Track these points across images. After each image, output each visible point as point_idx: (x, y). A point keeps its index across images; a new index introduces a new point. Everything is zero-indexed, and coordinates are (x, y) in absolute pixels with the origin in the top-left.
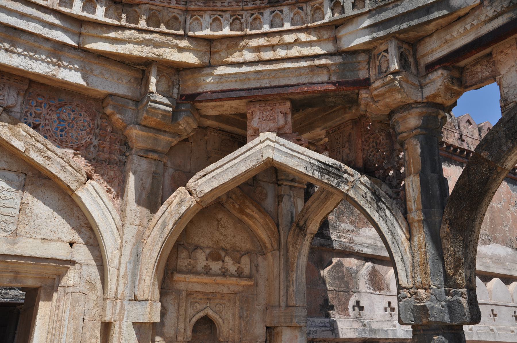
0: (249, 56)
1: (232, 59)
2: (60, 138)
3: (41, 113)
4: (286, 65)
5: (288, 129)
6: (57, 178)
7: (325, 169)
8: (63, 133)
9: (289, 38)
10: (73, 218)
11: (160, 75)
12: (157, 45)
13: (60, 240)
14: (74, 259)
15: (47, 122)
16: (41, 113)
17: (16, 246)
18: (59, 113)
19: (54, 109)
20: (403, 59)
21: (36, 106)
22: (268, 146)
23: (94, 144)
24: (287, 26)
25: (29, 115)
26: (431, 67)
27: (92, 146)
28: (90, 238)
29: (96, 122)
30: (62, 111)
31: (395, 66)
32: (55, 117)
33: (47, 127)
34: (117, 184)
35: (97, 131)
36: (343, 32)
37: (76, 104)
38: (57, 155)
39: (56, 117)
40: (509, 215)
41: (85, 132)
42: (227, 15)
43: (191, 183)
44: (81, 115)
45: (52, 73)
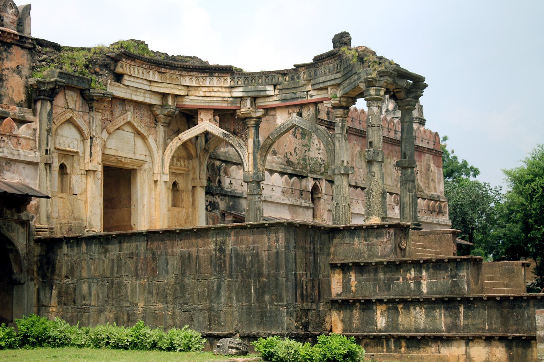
0: (202, 94)
4: (215, 99)
7: (225, 135)
9: (216, 89)
12: (172, 88)
20: (251, 103)
26: (260, 107)
31: (249, 106)
36: (234, 90)
40: (288, 139)
42: (194, 78)
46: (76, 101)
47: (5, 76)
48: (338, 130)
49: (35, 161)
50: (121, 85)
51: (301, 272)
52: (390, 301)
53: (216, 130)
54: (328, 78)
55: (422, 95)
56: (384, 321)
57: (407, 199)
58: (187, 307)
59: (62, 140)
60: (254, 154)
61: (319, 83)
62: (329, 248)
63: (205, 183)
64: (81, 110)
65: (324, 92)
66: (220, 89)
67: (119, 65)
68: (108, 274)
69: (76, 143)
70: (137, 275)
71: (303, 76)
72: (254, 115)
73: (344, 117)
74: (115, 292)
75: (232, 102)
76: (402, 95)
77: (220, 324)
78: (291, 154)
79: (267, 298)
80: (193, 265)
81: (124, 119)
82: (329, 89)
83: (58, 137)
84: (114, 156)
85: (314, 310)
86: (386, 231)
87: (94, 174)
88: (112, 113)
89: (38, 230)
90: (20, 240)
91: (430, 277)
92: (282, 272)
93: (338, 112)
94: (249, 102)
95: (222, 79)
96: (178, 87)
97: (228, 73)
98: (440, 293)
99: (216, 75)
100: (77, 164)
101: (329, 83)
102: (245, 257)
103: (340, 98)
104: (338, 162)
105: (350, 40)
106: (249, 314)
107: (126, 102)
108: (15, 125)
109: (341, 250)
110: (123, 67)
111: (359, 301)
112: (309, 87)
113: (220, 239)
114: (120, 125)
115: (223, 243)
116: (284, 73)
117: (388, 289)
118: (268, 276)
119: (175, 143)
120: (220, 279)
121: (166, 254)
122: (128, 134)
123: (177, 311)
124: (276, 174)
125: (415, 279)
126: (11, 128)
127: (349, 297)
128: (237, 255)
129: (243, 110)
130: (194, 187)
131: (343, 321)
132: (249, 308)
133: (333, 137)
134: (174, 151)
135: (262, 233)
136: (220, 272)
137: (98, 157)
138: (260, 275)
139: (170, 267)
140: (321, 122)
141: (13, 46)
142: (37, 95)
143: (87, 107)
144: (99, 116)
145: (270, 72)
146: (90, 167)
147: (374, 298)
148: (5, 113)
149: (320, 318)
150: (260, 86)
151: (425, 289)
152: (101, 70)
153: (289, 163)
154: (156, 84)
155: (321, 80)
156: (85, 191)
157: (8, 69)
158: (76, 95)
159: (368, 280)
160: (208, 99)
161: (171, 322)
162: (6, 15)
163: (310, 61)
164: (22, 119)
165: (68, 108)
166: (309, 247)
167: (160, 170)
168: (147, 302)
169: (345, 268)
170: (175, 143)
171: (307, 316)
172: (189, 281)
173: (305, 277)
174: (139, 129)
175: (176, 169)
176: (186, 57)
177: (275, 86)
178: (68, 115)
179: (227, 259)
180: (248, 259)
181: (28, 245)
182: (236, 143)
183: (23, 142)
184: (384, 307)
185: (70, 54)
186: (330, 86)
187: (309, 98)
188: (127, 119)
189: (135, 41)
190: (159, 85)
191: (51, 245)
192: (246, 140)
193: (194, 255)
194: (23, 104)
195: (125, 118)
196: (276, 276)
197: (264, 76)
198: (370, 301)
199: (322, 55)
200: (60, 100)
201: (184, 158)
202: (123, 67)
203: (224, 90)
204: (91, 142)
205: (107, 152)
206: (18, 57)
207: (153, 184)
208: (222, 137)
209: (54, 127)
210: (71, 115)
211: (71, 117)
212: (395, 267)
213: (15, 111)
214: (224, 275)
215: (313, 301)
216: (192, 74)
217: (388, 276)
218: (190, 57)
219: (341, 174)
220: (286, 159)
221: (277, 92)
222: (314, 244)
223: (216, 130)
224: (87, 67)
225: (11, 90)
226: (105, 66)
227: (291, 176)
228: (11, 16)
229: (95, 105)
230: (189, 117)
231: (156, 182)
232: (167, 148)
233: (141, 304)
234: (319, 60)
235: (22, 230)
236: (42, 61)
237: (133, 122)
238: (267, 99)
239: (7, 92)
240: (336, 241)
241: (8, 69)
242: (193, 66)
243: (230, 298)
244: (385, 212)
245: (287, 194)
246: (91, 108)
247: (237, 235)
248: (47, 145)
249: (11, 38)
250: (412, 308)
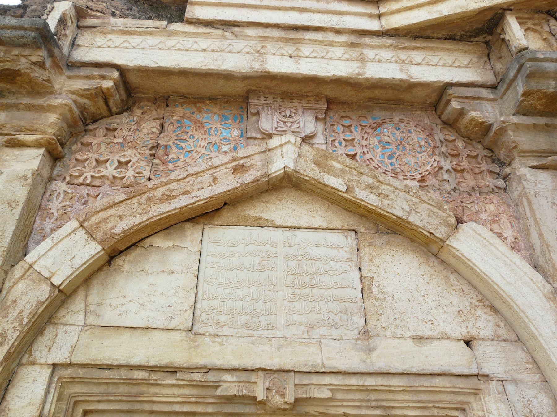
2: (391, 168)
3: (353, 139)
6: (408, 223)
8: (394, 160)
10: (453, 293)
13: (444, 337)
14: (485, 371)
15: (365, 150)
16: (353, 139)
17: (374, 354)
18: (379, 135)
19: (369, 130)
21: (343, 132)
23: (445, 168)
25: (337, 144)
27: (443, 171)
28: (498, 326)
29: (436, 137)
30: (382, 132)
32: (374, 141)
33: (368, 157)
34: (509, 224)
35: (443, 149)
37: (398, 119)
38: (396, 189)
39: (376, 141)
41: (425, 154)
44: (411, 133)
45: (357, 72)
84: (172, 370)
107: (253, 101)
188: (268, 162)
195: (257, 160)
237: (310, 171)
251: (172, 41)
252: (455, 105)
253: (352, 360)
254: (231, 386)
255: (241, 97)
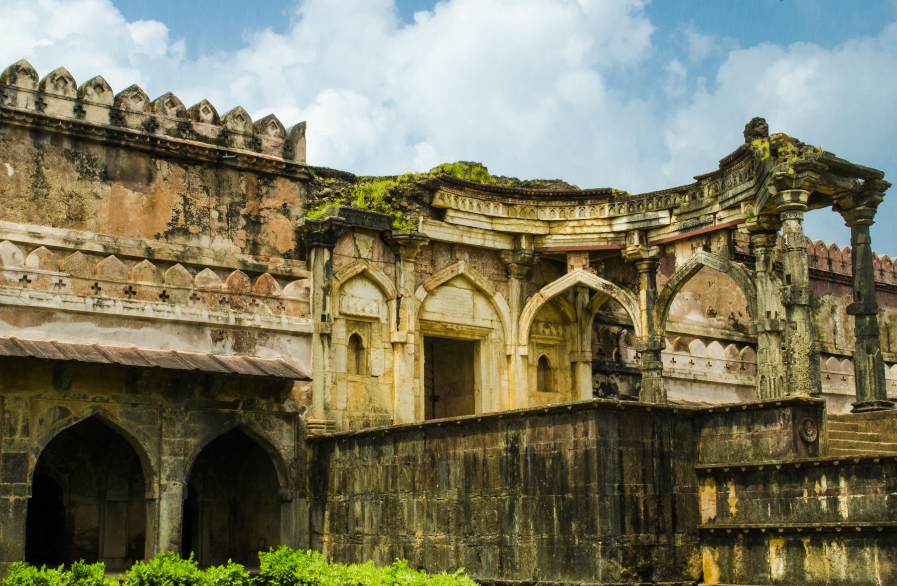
0: (569, 230)
1: (561, 232)
4: (588, 236)
5: (588, 266)
7: (606, 286)
9: (589, 223)
11: (526, 239)
20: (641, 240)
22: (580, 273)
24: (588, 217)
26: (653, 243)
36: (614, 222)
40: (735, 294)
42: (558, 209)
43: (542, 291)
46: (372, 248)
47: (264, 217)
48: (759, 267)
49: (306, 331)
50: (444, 224)
51: (633, 484)
52: (788, 532)
53: (594, 280)
54: (740, 188)
55: (882, 201)
56: (782, 566)
57: (867, 365)
58: (473, 540)
59: (352, 302)
60: (648, 311)
61: (729, 199)
62: (695, 444)
63: (589, 356)
64: (381, 259)
65: (737, 211)
66: (595, 223)
67: (438, 195)
68: (382, 486)
69: (375, 305)
70: (414, 490)
71: (708, 192)
72: (645, 255)
73: (769, 246)
74: (390, 517)
75: (614, 240)
76: (848, 202)
77: (513, 567)
78: (741, 315)
79: (574, 526)
80: (479, 473)
81: (452, 271)
82: (742, 205)
83: (345, 298)
84: (439, 322)
85: (664, 545)
86: (780, 412)
87: (403, 347)
88: (433, 263)
89: (310, 426)
90: (284, 442)
91: (853, 489)
92: (594, 484)
93: (758, 240)
94: (636, 237)
95: (597, 208)
96: (534, 223)
97: (605, 198)
98: (870, 518)
99: (589, 202)
100: (377, 334)
101: (741, 197)
102: (543, 460)
103: (758, 217)
104: (762, 314)
105: (766, 129)
106: (551, 552)
107: (456, 248)
108: (276, 283)
109: (713, 446)
110: (445, 198)
111: (741, 530)
112: (717, 207)
113: (511, 433)
114: (446, 279)
115: (516, 439)
116: (681, 191)
117: (787, 512)
118: (575, 491)
119: (535, 303)
120: (513, 496)
121: (448, 455)
122: (461, 291)
123: (462, 545)
124: (715, 344)
125: (828, 493)
126: (269, 287)
127: (728, 523)
128: (534, 456)
129: (630, 249)
130: (574, 364)
131: (719, 564)
132: (551, 541)
133: (755, 276)
134: (534, 312)
135: (565, 421)
136: (512, 485)
137: (410, 323)
138: (564, 489)
139: (452, 478)
140: (739, 257)
141: (278, 178)
142: (313, 240)
143: (392, 256)
144: (410, 267)
145: (663, 192)
146: (396, 338)
147: (764, 525)
148: (261, 267)
149: (676, 559)
150: (650, 213)
151: (844, 511)
152: (409, 204)
153: (738, 327)
154: (500, 221)
155: (730, 193)
156: (391, 371)
157: (268, 208)
158: (371, 241)
159: (754, 495)
160: (579, 237)
161: (453, 562)
162: (266, 137)
163: (716, 168)
164: (287, 274)
165: (360, 257)
166: (650, 441)
167: (514, 340)
168: (426, 530)
169: (719, 477)
170: (535, 303)
171: (647, 556)
172: (475, 498)
173: (642, 492)
174: (478, 283)
175: (543, 339)
176: (545, 181)
177: (671, 211)
178: (359, 268)
179: (522, 464)
180: (549, 463)
181: (297, 448)
182: (622, 296)
183: (290, 306)
184: (780, 542)
185: (367, 186)
186: (743, 201)
187: (717, 223)
188: (458, 270)
189: (466, 163)
190: (506, 222)
191: (323, 445)
192: (637, 294)
193: (481, 459)
194: (292, 255)
195: (456, 269)
196: (586, 490)
197: (655, 199)
198: (758, 530)
199: (728, 158)
200: (346, 248)
201: (556, 324)
202: (445, 198)
203: (601, 223)
204: (398, 304)
205: (426, 316)
206: (286, 191)
207: (505, 360)
208: (602, 289)
209: (336, 284)
210: (365, 267)
211: (364, 271)
212: (796, 473)
213: (281, 264)
214: (518, 489)
215: (659, 532)
216: (553, 203)
217: (785, 488)
218: (550, 181)
219: (766, 332)
220: (732, 322)
221: (674, 219)
222: (661, 438)
223: (594, 280)
224: (388, 200)
225: (272, 236)
226: (414, 198)
227: (740, 345)
228: (274, 139)
229: (403, 252)
230: (557, 263)
231: (509, 357)
232: (525, 310)
233: (419, 533)
234: (727, 164)
235: (286, 427)
236: (324, 196)
237: (467, 274)
238: (662, 231)
239: (267, 239)
240: (705, 431)
241: (268, 208)
242: (553, 193)
243: (525, 526)
244: (819, 385)
245: (735, 370)
246: (398, 258)
247: (533, 426)
248: (324, 308)
249: (272, 167)
250: (825, 544)
251: (442, 229)
252: (503, 256)
253: (470, 322)
254: (449, 326)
255: (452, 247)
